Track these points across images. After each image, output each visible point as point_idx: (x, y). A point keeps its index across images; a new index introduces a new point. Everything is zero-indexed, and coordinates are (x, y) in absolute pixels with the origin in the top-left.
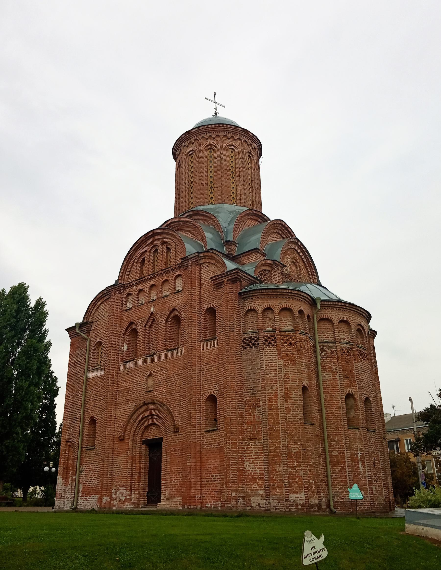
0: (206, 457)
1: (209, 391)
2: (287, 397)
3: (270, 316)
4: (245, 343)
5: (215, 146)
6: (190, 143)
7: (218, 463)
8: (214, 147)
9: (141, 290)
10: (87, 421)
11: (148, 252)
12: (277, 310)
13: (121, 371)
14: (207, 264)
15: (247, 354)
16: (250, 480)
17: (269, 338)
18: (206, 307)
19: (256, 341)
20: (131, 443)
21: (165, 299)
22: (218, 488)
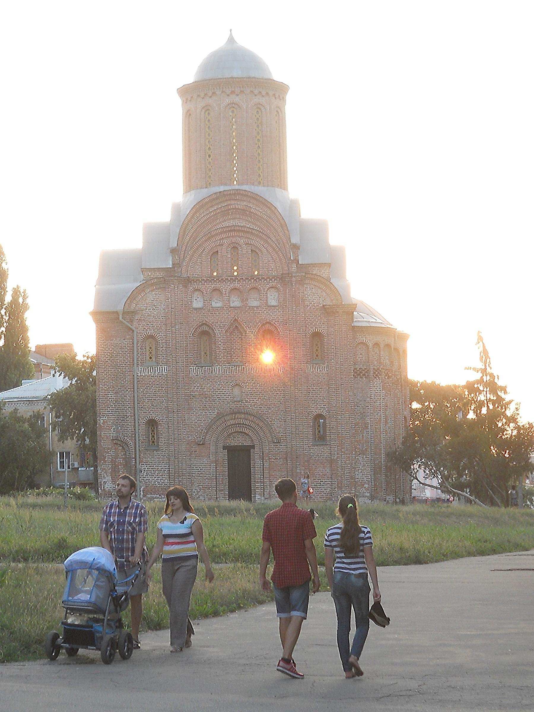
0: (313, 466)
1: (317, 410)
2: (386, 422)
3: (377, 350)
4: (356, 373)
5: (263, 106)
6: (233, 92)
7: (328, 471)
8: (262, 108)
9: (215, 290)
10: (143, 421)
11: (224, 247)
12: (382, 346)
13: (192, 374)
14: (312, 286)
15: (358, 383)
16: (359, 486)
17: (376, 371)
18: (312, 330)
19: (366, 372)
20: (212, 448)
21: (255, 309)
22: (328, 491)
